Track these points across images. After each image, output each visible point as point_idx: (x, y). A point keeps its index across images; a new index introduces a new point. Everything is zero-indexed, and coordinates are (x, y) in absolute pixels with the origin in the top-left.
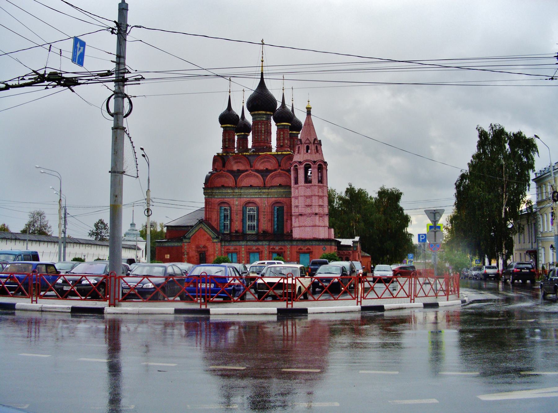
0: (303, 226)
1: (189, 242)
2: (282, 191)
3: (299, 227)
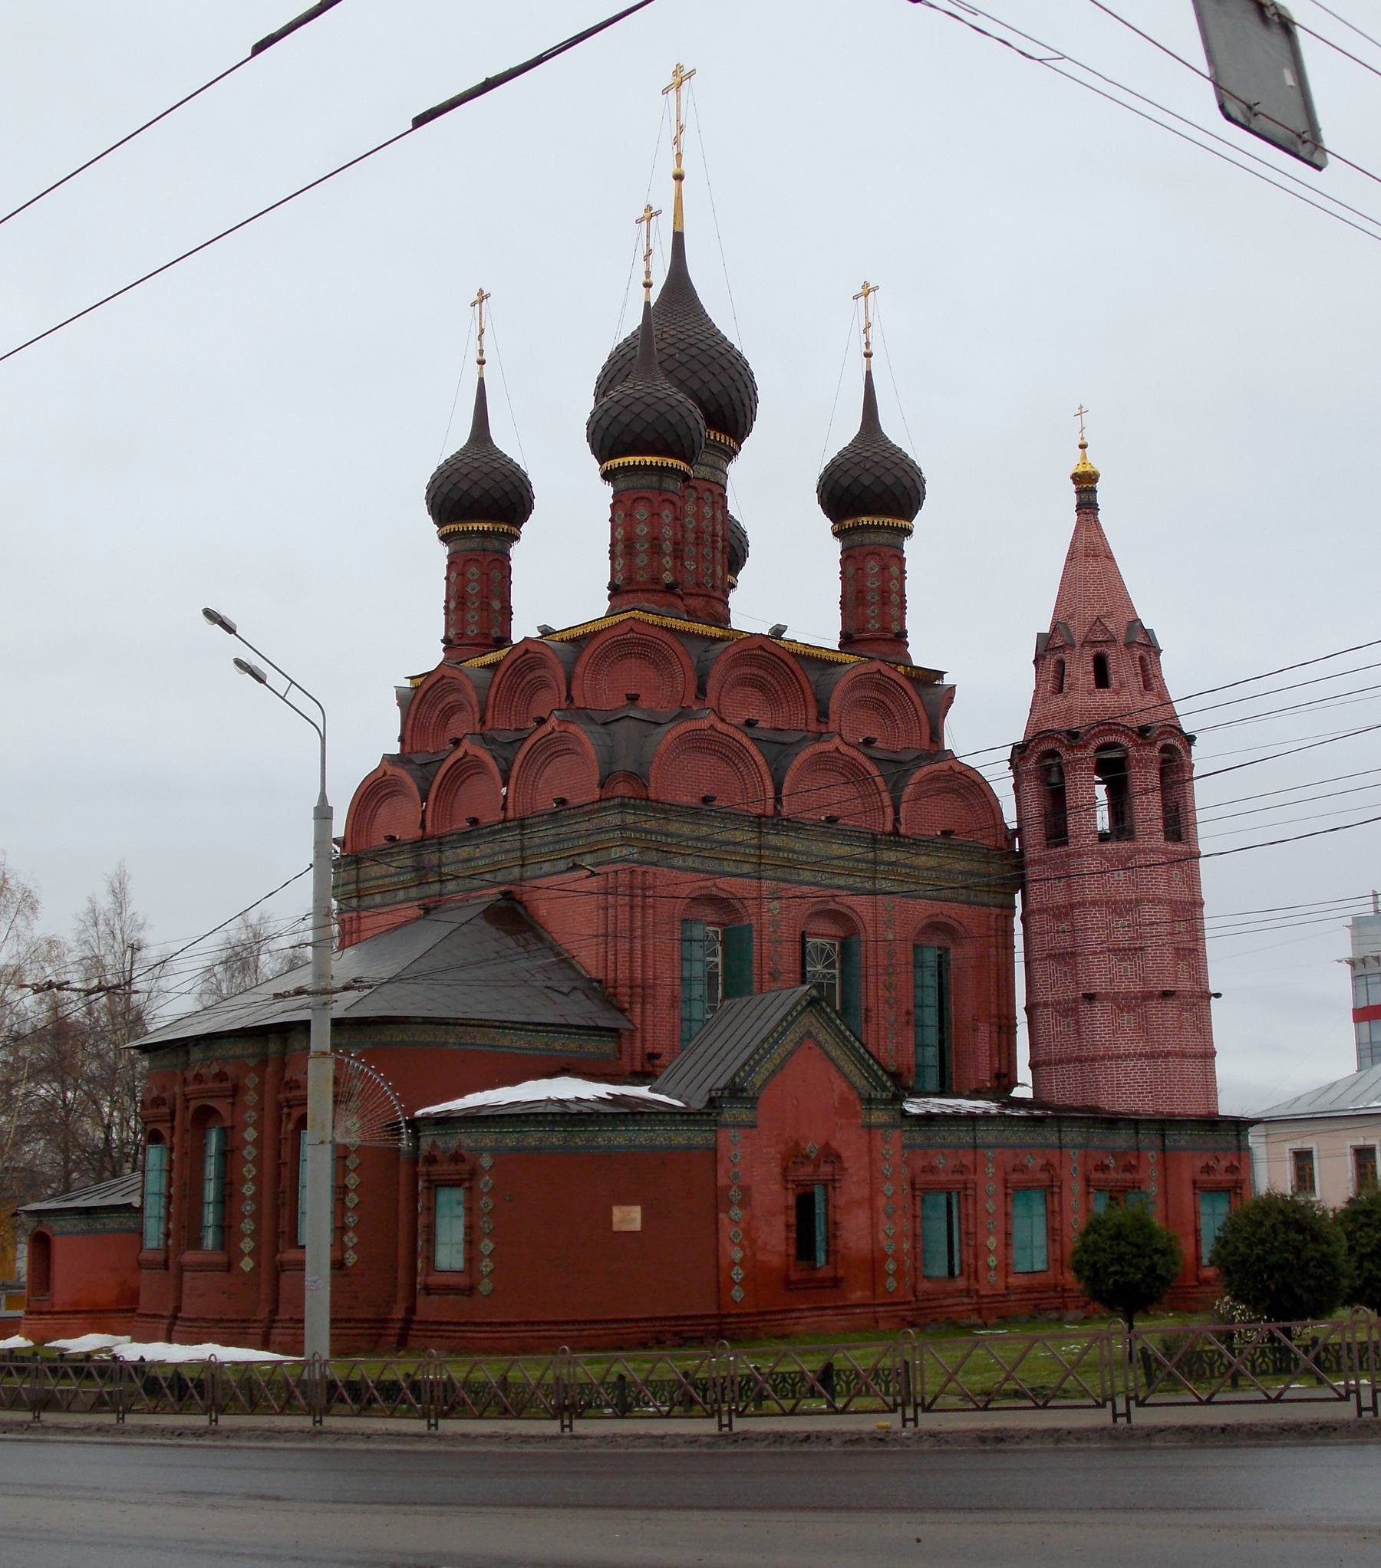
0: (1176, 1054)
1: (753, 1126)
2: (961, 866)
3: (1151, 1056)
